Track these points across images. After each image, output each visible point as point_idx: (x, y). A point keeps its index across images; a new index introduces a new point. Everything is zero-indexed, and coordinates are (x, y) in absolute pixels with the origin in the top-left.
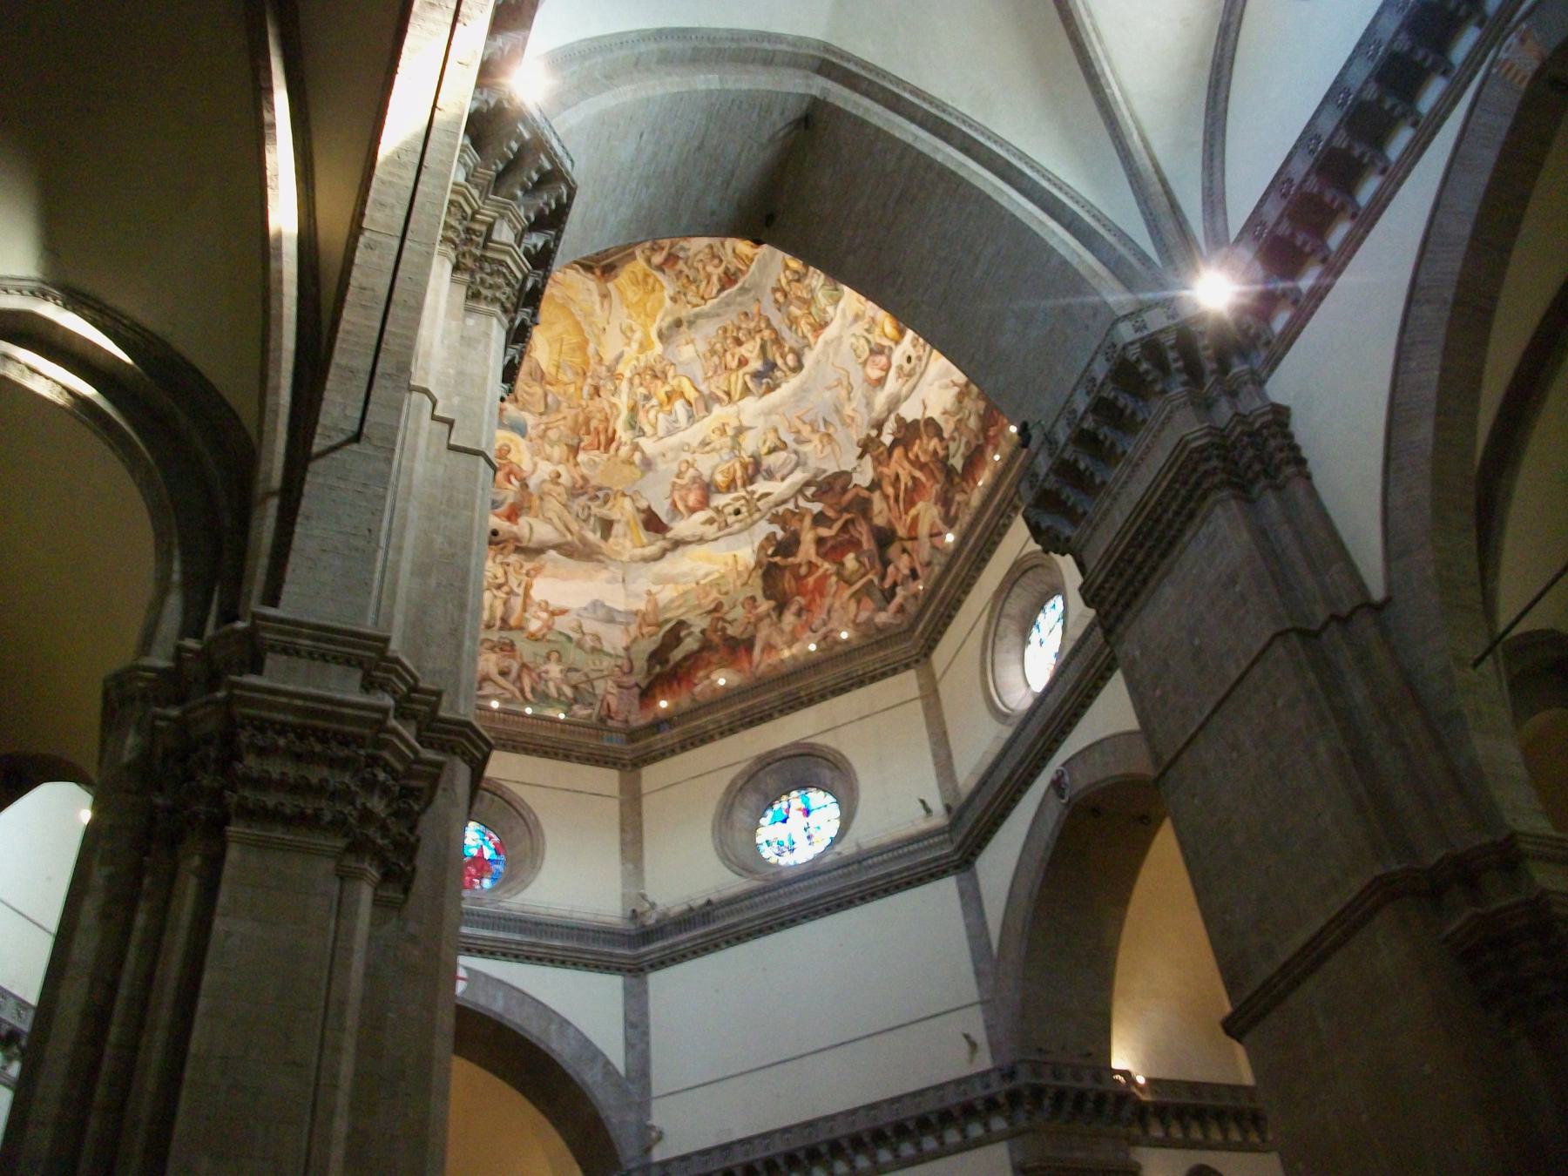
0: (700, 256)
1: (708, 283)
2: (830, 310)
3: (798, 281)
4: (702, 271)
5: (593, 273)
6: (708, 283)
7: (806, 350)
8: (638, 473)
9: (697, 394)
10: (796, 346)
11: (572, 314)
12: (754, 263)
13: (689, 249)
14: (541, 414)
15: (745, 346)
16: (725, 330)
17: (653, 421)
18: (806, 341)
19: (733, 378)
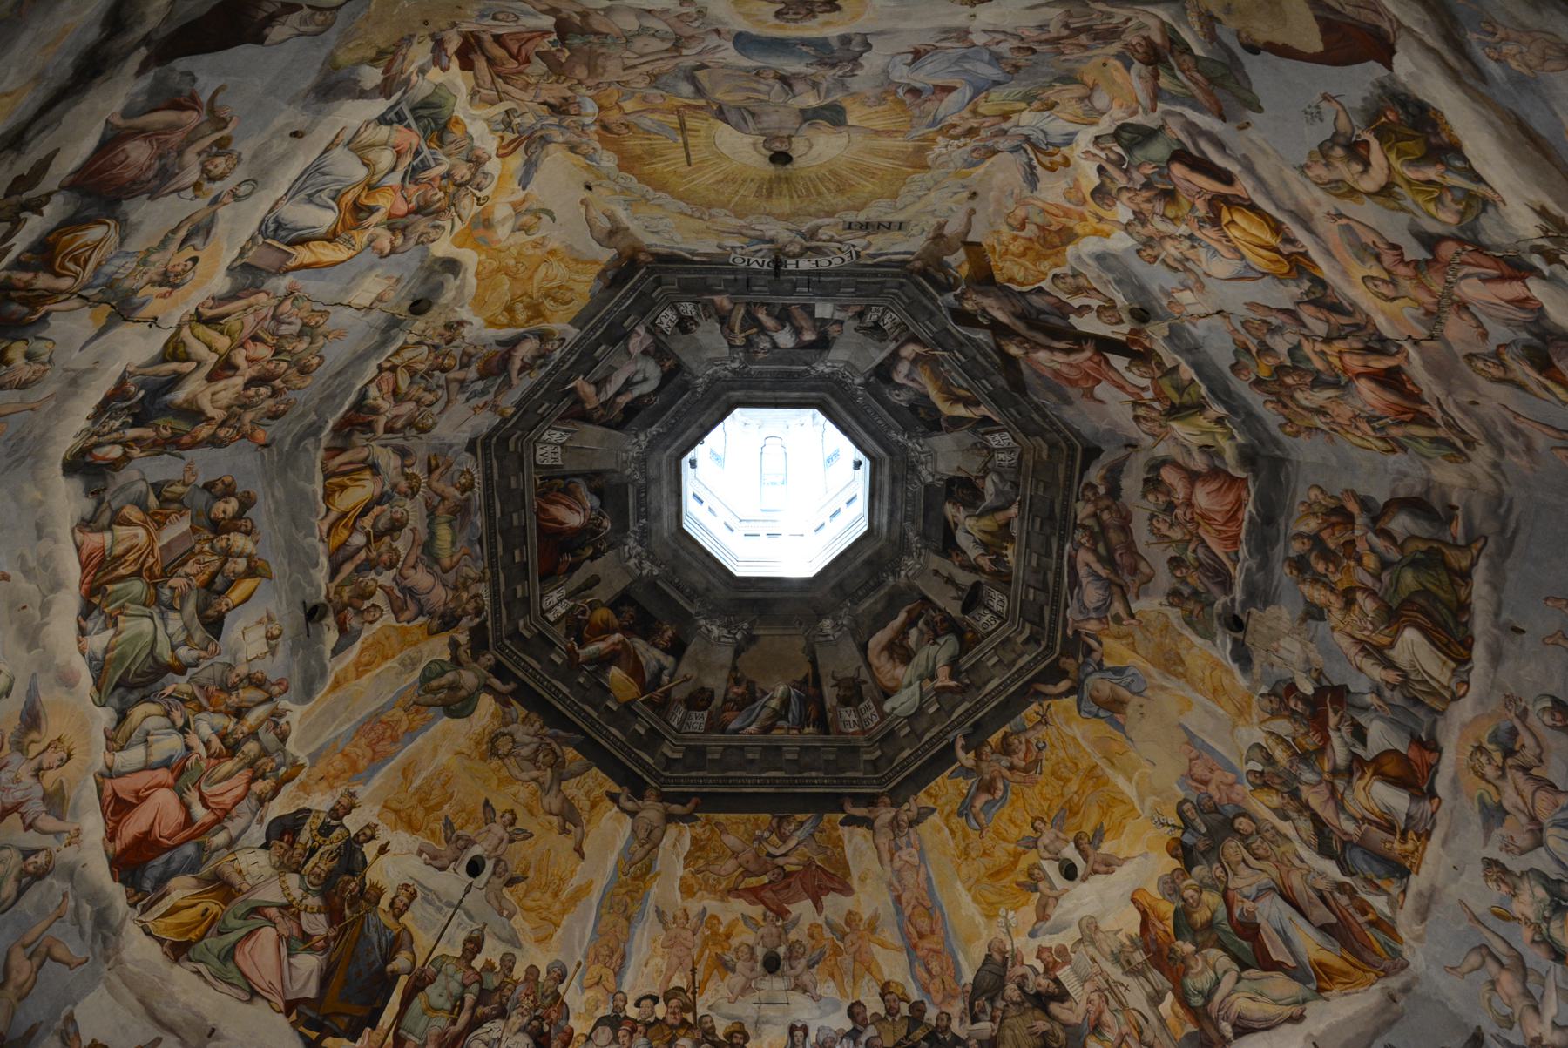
0: (436, 409)
1: (395, 392)
2: (98, 641)
3: (208, 585)
4: (420, 393)
5: (652, 254)
6: (395, 392)
7: (87, 505)
8: (343, 57)
9: (291, 263)
10: (121, 478)
11: (681, 199)
12: (320, 492)
13: (468, 400)
14: (703, 66)
15: (240, 388)
16: (304, 371)
17: (372, 155)
18: (105, 518)
19: (223, 343)
